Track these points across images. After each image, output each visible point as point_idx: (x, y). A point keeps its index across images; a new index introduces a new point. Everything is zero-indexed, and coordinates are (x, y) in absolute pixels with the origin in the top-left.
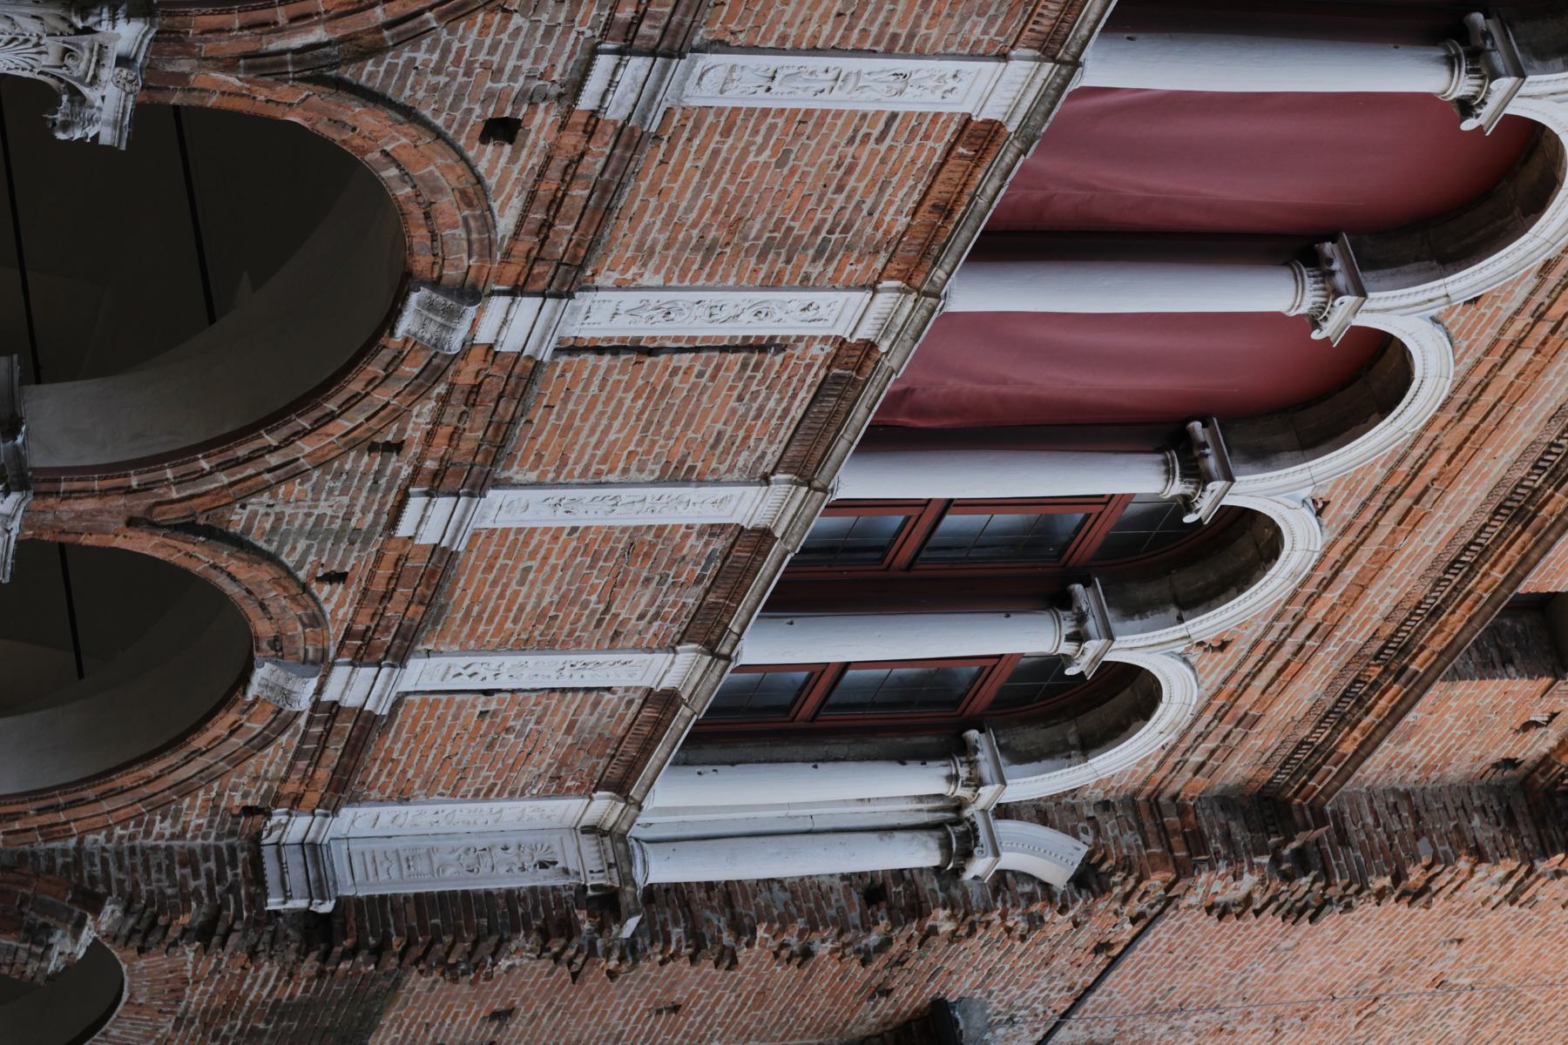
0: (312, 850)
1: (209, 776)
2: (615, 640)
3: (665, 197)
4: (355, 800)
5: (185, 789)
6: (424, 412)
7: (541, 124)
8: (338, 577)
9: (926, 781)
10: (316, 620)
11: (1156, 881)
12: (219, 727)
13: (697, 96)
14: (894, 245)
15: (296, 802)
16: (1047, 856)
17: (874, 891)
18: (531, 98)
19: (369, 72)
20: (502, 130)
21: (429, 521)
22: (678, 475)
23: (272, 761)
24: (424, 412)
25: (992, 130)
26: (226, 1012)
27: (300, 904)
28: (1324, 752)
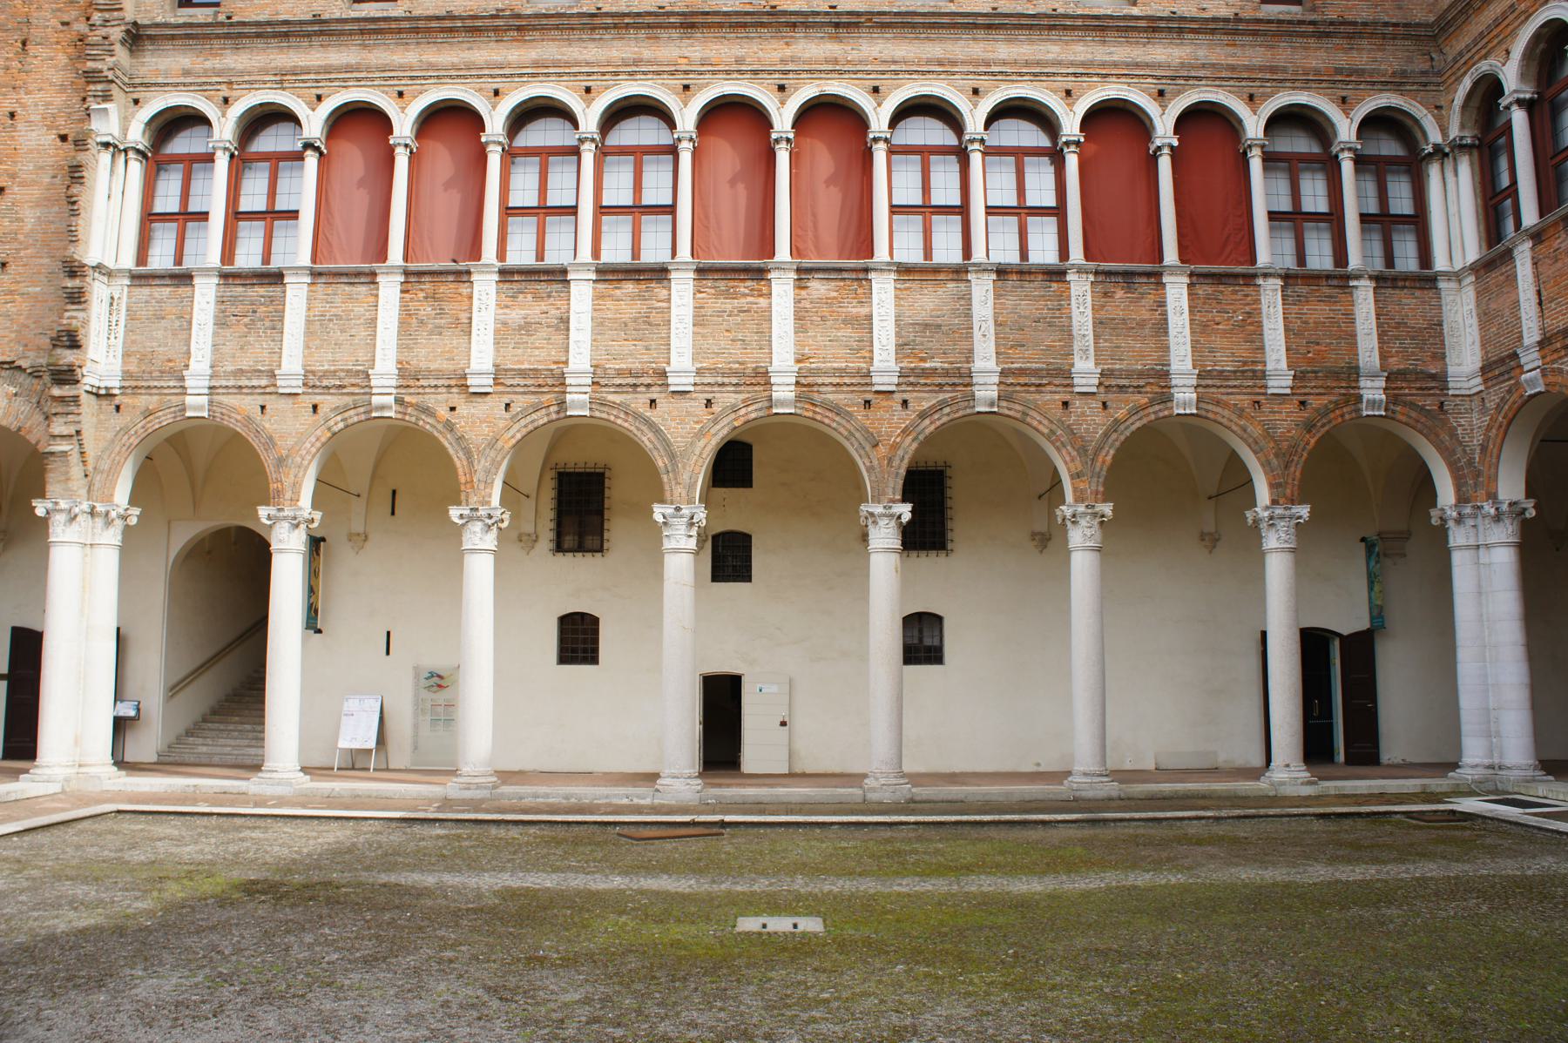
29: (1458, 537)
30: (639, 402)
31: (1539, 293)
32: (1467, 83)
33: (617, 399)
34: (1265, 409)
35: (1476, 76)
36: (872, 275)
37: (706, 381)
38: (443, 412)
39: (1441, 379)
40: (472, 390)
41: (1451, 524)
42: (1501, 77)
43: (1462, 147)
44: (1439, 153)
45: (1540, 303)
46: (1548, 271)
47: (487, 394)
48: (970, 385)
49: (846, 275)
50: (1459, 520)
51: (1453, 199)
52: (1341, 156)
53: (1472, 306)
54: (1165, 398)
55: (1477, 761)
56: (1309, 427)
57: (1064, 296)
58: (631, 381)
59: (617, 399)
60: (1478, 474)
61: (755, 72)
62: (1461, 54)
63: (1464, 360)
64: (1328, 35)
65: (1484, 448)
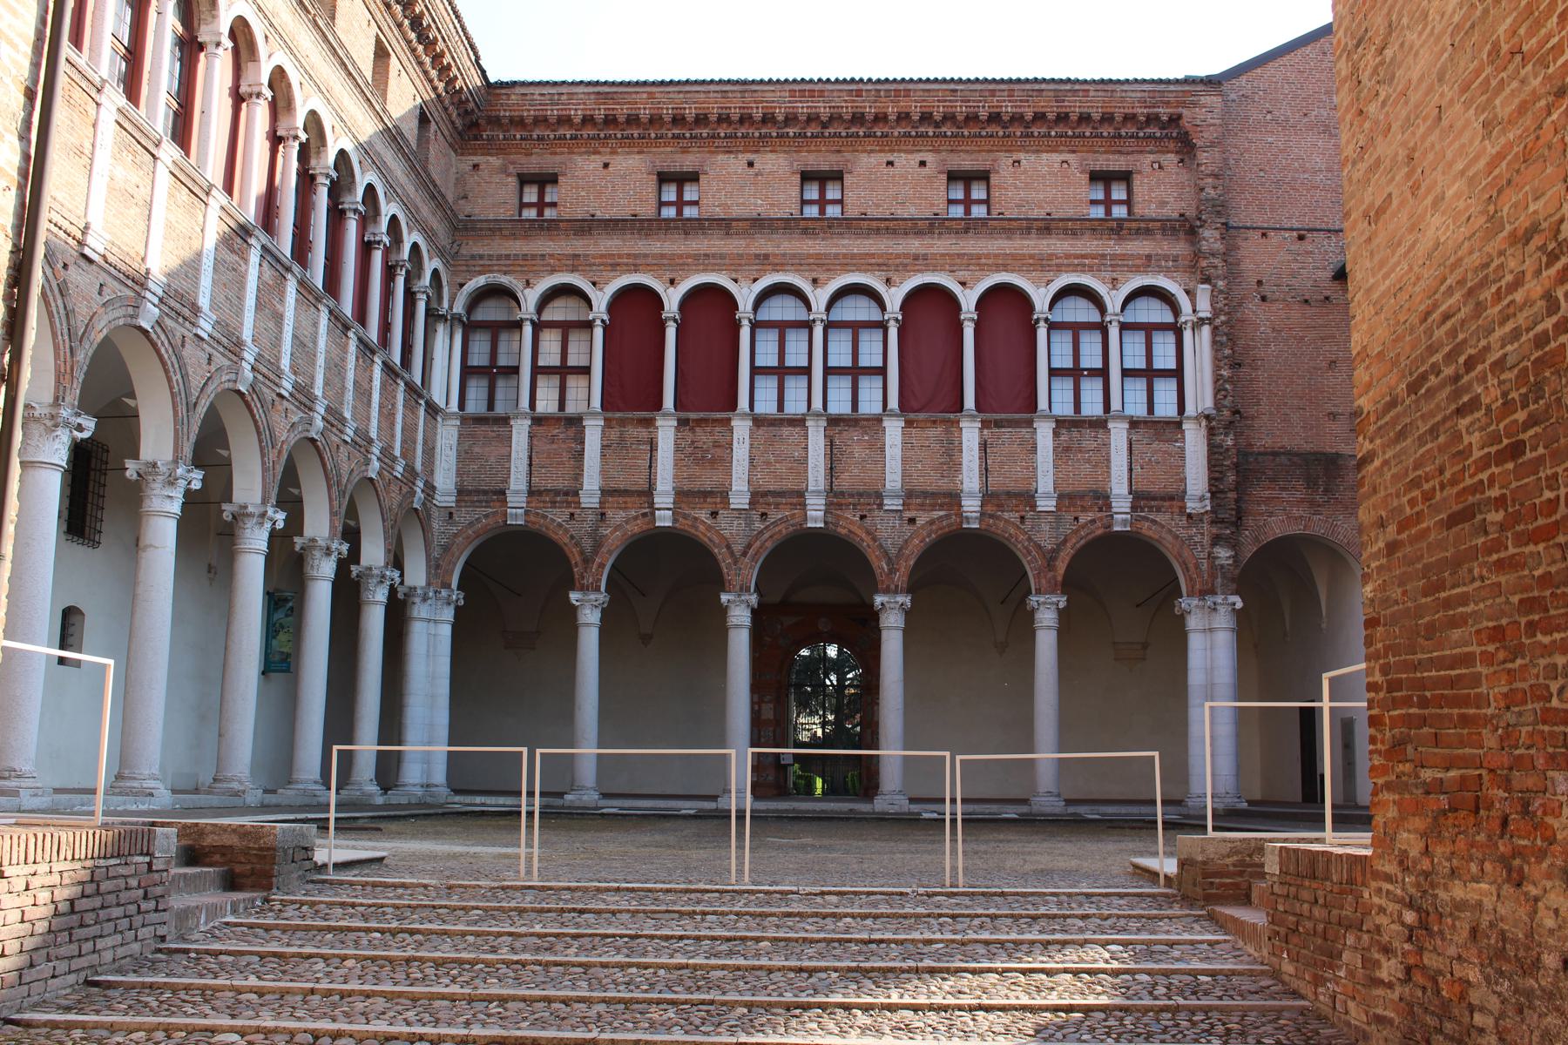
0: (1202, 499)
1: (1170, 531)
2: (1107, 445)
3: (933, 481)
4: (1185, 492)
5: (1176, 537)
6: (1006, 515)
7: (908, 514)
8: (1076, 519)
9: (1187, 335)
10: (1093, 521)
11: (1204, 263)
12: (1150, 533)
13: (899, 485)
14: (947, 431)
15: (1183, 508)
16: (1204, 291)
17: (1214, 342)
18: (901, 518)
19: (893, 551)
20: (912, 521)
21: (1046, 504)
22: (1034, 449)
23: (1159, 518)
24: (1006, 515)
25: (906, 422)
26: (1312, 503)
27: (1208, 502)
28: (1163, 229)
29: (420, 610)
30: (179, 331)
31: (530, 458)
32: (481, 281)
33: (169, 322)
34: (393, 487)
35: (491, 280)
36: (289, 276)
37: (215, 334)
38: (60, 266)
39: (433, 488)
40: (87, 251)
41: (417, 600)
42: (519, 295)
43: (460, 321)
44: (443, 318)
45: (530, 465)
46: (541, 445)
47: (90, 261)
48: (310, 409)
49: (279, 267)
50: (425, 599)
51: (446, 353)
52: (419, 296)
53: (454, 441)
54: (367, 462)
55: (417, 781)
56: (400, 505)
57: (344, 349)
58: (178, 306)
59: (169, 322)
60: (438, 567)
61: (260, 8)
62: (481, 257)
63: (445, 480)
64: (433, 197)
65: (446, 549)
